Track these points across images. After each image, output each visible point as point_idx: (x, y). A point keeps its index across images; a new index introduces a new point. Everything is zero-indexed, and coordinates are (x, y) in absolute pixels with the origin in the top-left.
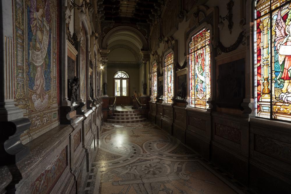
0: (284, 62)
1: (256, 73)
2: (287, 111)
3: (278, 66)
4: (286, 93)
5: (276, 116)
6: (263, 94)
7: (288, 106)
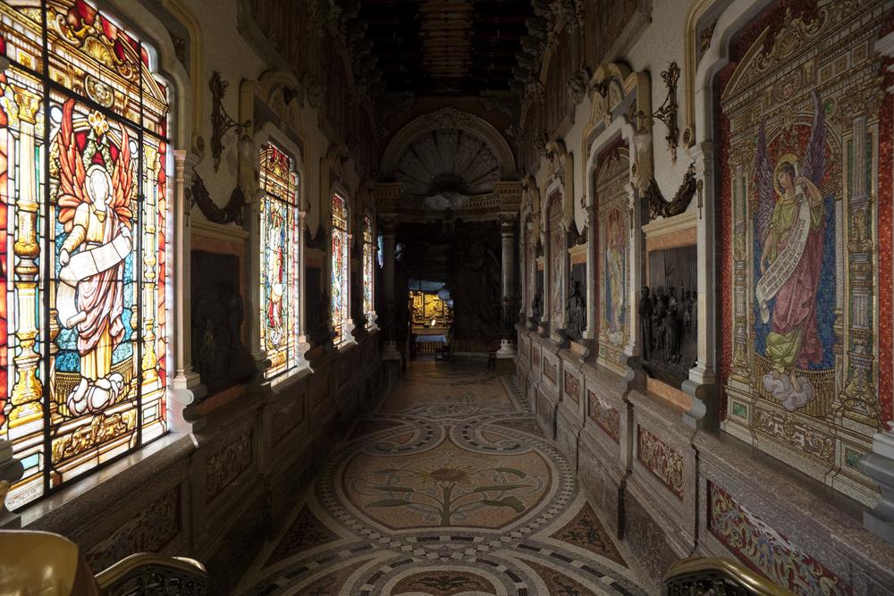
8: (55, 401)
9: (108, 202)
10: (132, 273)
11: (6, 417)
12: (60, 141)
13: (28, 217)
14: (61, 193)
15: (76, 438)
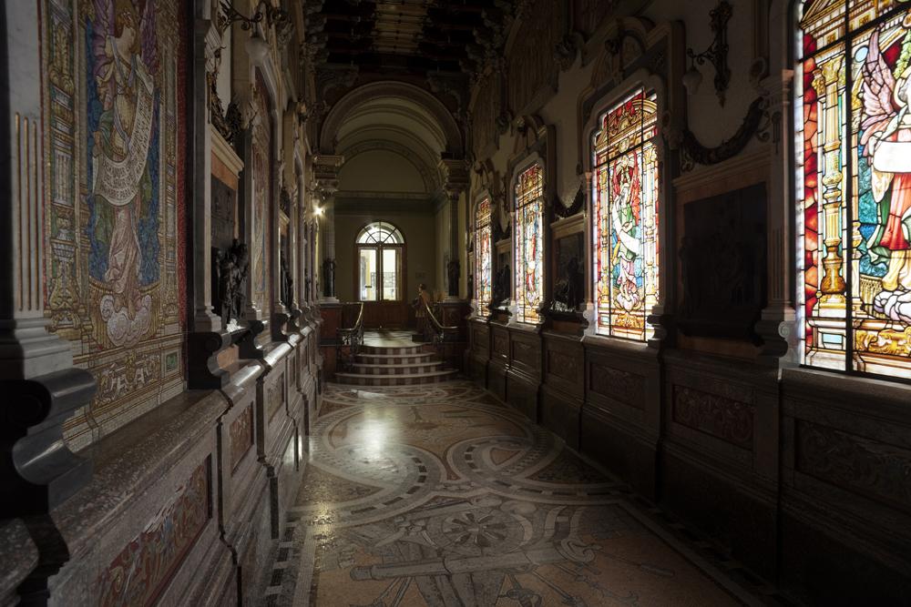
0: (889, 194)
1: (801, 230)
2: (899, 348)
3: (869, 207)
4: (897, 290)
5: (865, 362)
6: (823, 294)
7: (903, 331)
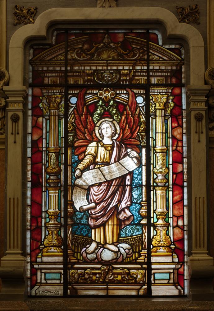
5: (76, 289)
8: (72, 249)
9: (115, 138)
10: (141, 180)
11: (41, 251)
12: (76, 113)
13: (53, 155)
14: (76, 140)
15: (87, 273)
